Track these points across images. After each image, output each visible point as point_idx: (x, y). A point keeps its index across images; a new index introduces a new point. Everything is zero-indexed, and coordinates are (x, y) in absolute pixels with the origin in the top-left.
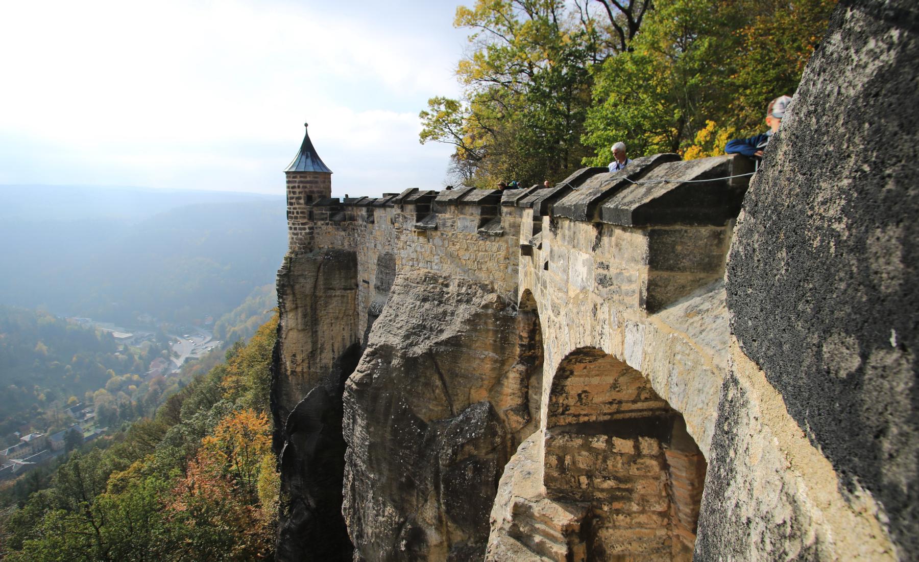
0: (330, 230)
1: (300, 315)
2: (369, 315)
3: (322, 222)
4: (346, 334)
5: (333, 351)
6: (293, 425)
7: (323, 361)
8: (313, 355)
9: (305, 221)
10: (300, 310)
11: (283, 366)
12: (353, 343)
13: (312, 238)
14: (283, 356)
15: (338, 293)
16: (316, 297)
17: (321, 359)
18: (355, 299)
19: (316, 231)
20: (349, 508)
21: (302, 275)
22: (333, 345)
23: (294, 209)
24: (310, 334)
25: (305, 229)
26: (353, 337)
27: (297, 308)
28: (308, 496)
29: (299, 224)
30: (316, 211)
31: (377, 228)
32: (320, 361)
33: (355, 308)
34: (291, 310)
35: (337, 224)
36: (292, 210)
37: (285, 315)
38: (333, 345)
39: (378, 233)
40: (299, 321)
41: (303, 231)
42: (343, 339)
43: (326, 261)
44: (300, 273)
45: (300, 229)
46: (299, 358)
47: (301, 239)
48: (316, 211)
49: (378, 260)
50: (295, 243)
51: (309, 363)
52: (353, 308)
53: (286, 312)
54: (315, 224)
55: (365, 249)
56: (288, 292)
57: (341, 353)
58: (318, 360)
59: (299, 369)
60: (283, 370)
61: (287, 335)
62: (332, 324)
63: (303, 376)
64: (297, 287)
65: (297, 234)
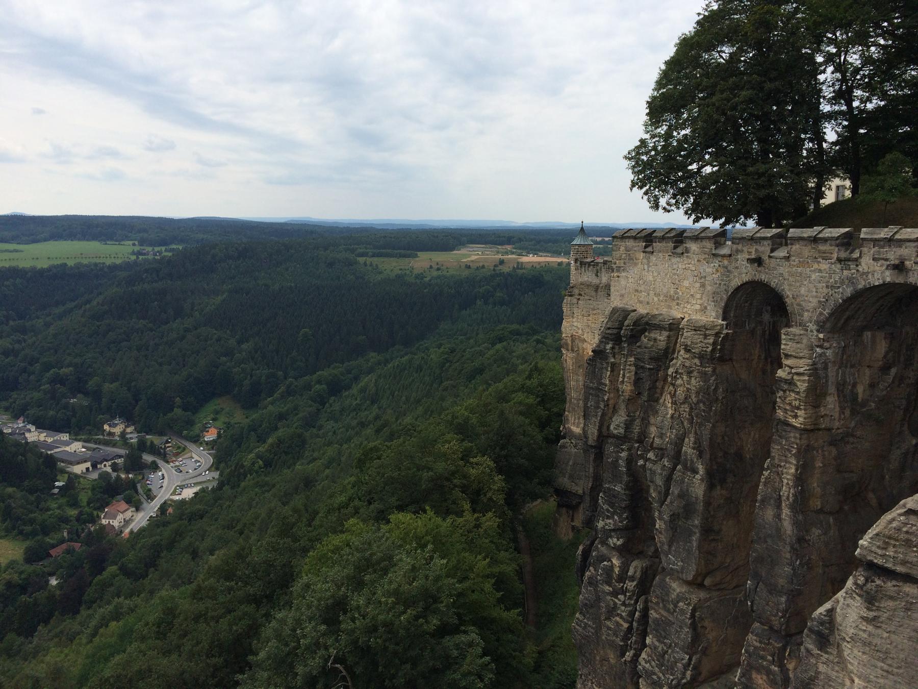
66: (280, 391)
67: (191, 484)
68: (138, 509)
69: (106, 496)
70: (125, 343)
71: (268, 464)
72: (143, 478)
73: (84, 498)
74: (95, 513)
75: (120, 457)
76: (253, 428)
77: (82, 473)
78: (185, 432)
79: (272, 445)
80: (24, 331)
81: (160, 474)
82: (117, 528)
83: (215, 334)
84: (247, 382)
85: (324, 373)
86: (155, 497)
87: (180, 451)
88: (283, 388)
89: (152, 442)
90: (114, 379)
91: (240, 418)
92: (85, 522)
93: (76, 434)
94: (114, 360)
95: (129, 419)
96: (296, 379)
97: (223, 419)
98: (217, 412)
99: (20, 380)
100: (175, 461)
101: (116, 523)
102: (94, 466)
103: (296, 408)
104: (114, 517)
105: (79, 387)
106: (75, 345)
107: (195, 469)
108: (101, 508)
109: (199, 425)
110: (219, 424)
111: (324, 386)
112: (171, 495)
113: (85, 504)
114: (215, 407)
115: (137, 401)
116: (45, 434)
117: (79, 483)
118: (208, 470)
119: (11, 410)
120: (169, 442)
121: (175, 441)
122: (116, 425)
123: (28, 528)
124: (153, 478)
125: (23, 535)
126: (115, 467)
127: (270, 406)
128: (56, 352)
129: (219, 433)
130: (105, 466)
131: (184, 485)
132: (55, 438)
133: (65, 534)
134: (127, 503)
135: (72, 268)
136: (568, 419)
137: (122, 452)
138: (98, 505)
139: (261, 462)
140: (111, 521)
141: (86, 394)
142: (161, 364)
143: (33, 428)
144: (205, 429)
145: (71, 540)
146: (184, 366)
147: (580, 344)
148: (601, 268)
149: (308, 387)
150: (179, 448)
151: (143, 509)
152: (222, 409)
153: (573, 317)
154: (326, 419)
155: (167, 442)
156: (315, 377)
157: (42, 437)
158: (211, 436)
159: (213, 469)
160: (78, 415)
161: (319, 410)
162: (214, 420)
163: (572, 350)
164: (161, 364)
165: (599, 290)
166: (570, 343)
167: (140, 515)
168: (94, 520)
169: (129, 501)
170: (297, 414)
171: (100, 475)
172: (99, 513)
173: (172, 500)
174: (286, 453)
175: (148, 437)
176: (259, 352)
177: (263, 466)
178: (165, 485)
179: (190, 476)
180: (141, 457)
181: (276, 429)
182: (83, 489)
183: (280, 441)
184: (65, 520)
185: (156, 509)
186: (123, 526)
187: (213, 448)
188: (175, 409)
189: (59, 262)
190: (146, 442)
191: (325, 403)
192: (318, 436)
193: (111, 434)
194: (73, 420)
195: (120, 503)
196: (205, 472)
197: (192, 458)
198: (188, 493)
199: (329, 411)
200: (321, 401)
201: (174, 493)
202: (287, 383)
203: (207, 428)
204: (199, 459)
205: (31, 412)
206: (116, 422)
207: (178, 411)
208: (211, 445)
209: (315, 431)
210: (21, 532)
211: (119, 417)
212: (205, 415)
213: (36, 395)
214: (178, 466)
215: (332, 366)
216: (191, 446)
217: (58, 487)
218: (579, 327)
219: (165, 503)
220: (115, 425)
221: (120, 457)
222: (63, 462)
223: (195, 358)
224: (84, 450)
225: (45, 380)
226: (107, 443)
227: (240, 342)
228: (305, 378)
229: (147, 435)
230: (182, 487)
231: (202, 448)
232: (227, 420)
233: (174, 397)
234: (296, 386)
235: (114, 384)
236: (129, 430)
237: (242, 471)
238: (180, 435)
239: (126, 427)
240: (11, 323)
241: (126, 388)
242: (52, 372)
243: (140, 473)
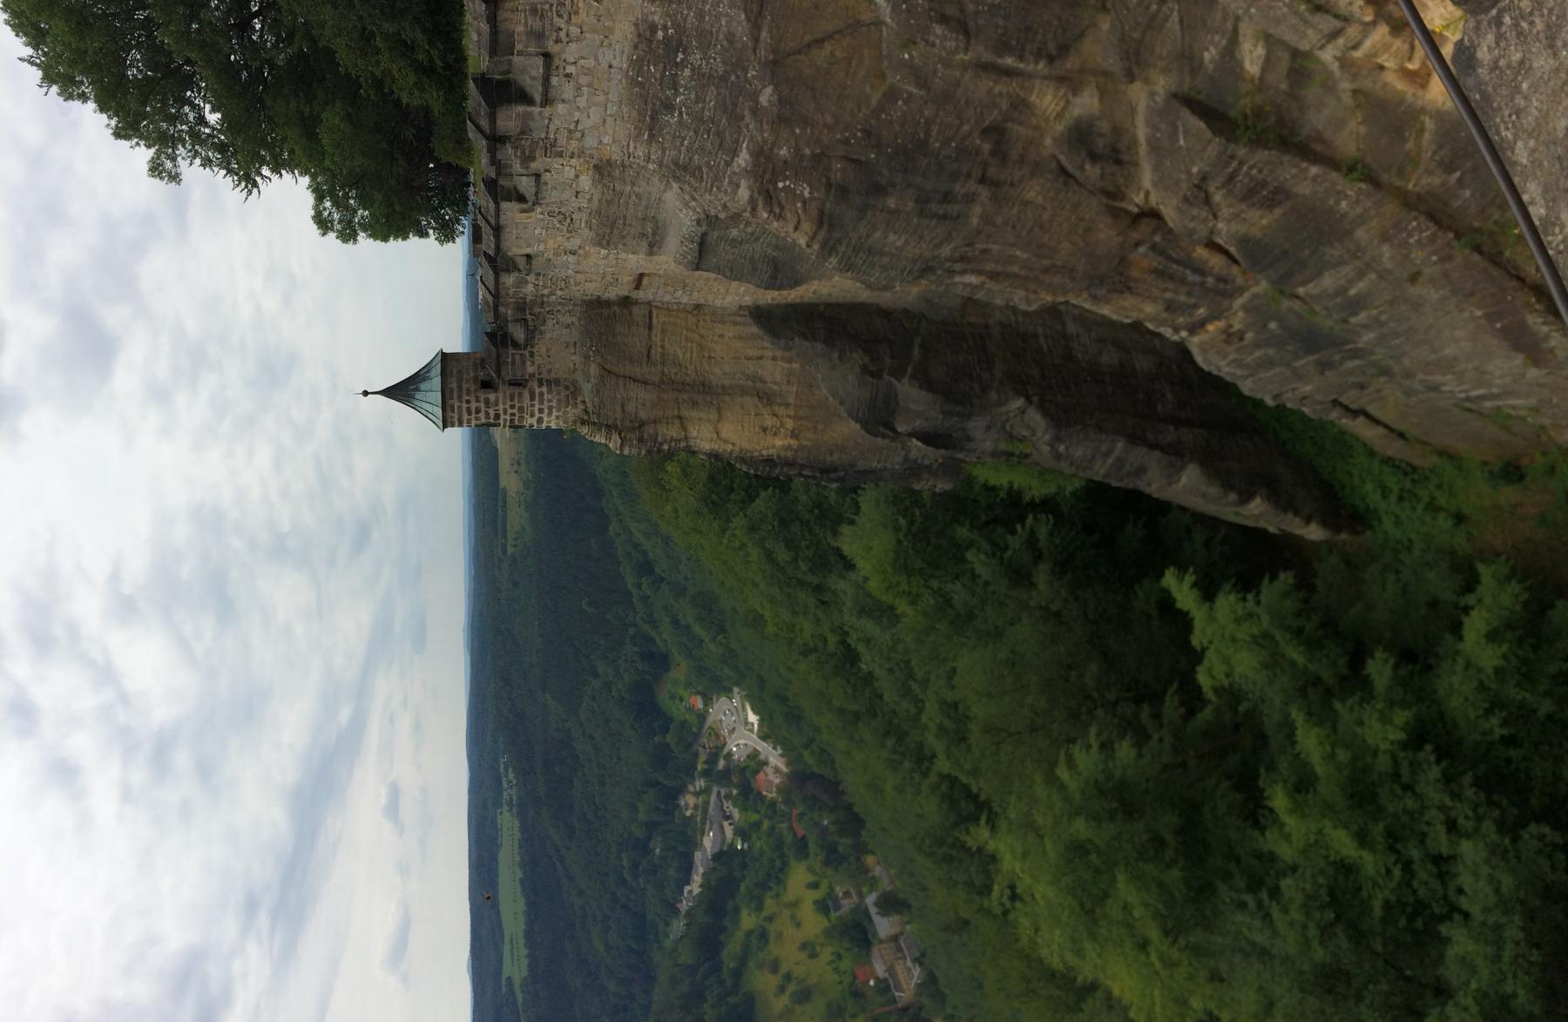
0: (543, 349)
1: (694, 414)
2: (697, 269)
3: (528, 363)
4: (730, 331)
5: (760, 358)
6: (881, 429)
7: (778, 377)
8: (766, 398)
9: (526, 394)
10: (684, 413)
11: (783, 453)
12: (749, 320)
13: (557, 382)
14: (764, 453)
15: (657, 339)
16: (662, 382)
17: (775, 383)
18: (669, 309)
19: (545, 376)
20: (1026, 289)
21: (623, 407)
22: (749, 359)
23: (505, 412)
24: (727, 398)
25: (541, 394)
26: (739, 319)
27: (680, 417)
28: (1003, 409)
29: (533, 406)
30: (508, 374)
31: (542, 247)
32: (778, 384)
33: (685, 311)
34: (685, 429)
35: (532, 334)
36: (508, 417)
37: (692, 442)
38: (749, 359)
39: (551, 244)
40: (703, 415)
41: (546, 397)
42: (739, 338)
43: (599, 359)
44: (618, 408)
45: (541, 402)
46: (769, 421)
47: (559, 401)
48: (508, 374)
49: (600, 245)
50: (566, 413)
51: (780, 405)
52: (681, 315)
53: (686, 438)
54: (532, 375)
55: (579, 277)
56: (651, 431)
57: (766, 344)
58: (775, 388)
59: (790, 424)
60: (789, 454)
61: (726, 442)
62: (710, 357)
63: (801, 418)
64: (643, 415)
65: (550, 408)
66: (650, 631)
71: (722, 629)
78: (694, 729)
81: (734, 749)
84: (640, 666)
85: (630, 580)
86: (755, 750)
88: (646, 627)
89: (705, 763)
91: (680, 670)
95: (680, 790)
97: (681, 692)
98: (672, 697)
108: (762, 798)
110: (685, 694)
111: (643, 579)
115: (658, 783)
123: (778, 863)
125: (783, 868)
127: (664, 636)
133: (784, 825)
139: (720, 637)
144: (691, 709)
149: (645, 598)
150: (710, 734)
152: (669, 692)
155: (704, 747)
156: (634, 591)
158: (699, 703)
159: (730, 695)
162: (681, 699)
167: (771, 759)
168: (773, 804)
173: (758, 731)
175: (699, 768)
185: (765, 745)
187: (711, 699)
189: (519, 889)
193: (696, 807)
198: (753, 718)
208: (708, 700)
210: (782, 870)
212: (676, 710)
216: (710, 721)
217: (743, 845)
220: (687, 804)
226: (705, 811)
227: (596, 675)
228: (635, 600)
230: (746, 723)
238: (697, 736)
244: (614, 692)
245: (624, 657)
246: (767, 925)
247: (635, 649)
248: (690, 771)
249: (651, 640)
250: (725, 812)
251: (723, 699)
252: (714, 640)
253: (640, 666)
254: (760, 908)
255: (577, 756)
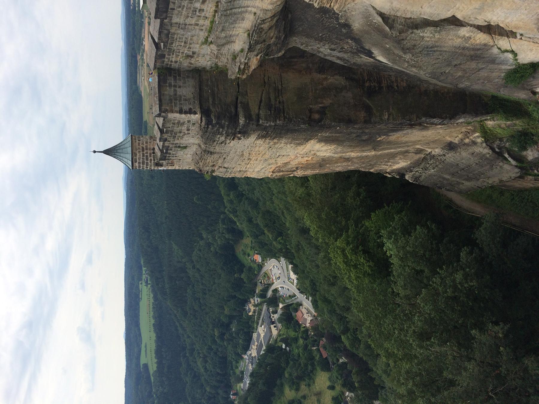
67: (288, 273)
68: (301, 305)
69: (292, 322)
70: (201, 301)
71: (280, 234)
72: (282, 298)
73: (292, 334)
74: (302, 329)
75: (268, 309)
76: (256, 236)
77: (277, 330)
79: (269, 231)
80: (193, 350)
81: (280, 289)
82: (312, 318)
83: (196, 252)
86: (294, 294)
87: (266, 275)
88: (231, 216)
89: (261, 291)
90: (222, 308)
91: (247, 241)
92: (308, 336)
93: (254, 328)
94: (211, 307)
95: (246, 301)
96: (226, 207)
97: (248, 251)
98: (244, 254)
99: (221, 355)
100: (272, 279)
101: (309, 319)
102: (273, 323)
103: (245, 212)
104: (306, 320)
105: (227, 326)
106: (202, 327)
107: (278, 269)
108: (299, 325)
109: (251, 264)
110: (251, 253)
112: (293, 285)
113: (296, 334)
114: (241, 254)
115: (235, 297)
116: (253, 346)
117: (283, 334)
118: (279, 262)
119: (238, 360)
120: (261, 281)
121: (260, 278)
122: (249, 308)
123: (310, 367)
124: (281, 292)
126: (275, 312)
128: (205, 337)
129: (257, 254)
130: (273, 317)
131: (288, 277)
132: (255, 341)
133: (314, 348)
134: (297, 311)
135: (155, 321)
136: (380, 170)
137: (265, 307)
138: (297, 327)
139: (279, 238)
140: (308, 321)
141: (230, 323)
142: (214, 283)
143: (249, 353)
144: (254, 261)
145: (318, 346)
146: (216, 270)
147: (290, 166)
148: (173, 144)
149: (231, 202)
150: (265, 276)
151: (301, 302)
152: (242, 250)
153: (246, 171)
154: (253, 195)
155: (261, 282)
157: (254, 347)
160: (243, 328)
161: (247, 198)
162: (249, 255)
163: (294, 171)
164: (214, 283)
165: (212, 150)
166: (281, 173)
168: (306, 331)
169: (296, 310)
170: (249, 212)
171: (279, 323)
172: (302, 326)
174: (274, 223)
175: (257, 292)
176: (208, 228)
177: (282, 237)
178: (287, 287)
179: (282, 271)
180: (269, 298)
181: (257, 224)
182: (287, 333)
183: (266, 226)
184: (306, 347)
185: (302, 295)
186: (311, 314)
188: (242, 277)
190: (261, 294)
191: (243, 193)
192: (265, 203)
193: (254, 312)
194: (245, 330)
195: (297, 315)
196: (281, 264)
197: (271, 270)
198: (293, 276)
199: (247, 192)
200: (240, 196)
201: (293, 283)
202: (228, 213)
203: (253, 260)
204: (272, 266)
205: (239, 351)
206: (248, 308)
207: (243, 276)
209: (261, 204)
210: (312, 372)
211: (245, 306)
212: (246, 260)
213: (230, 348)
214: (276, 278)
215: (218, 185)
216: (264, 269)
218: (263, 167)
219: (299, 289)
220: (250, 309)
221: (268, 309)
222: (270, 340)
223: (211, 264)
224: (263, 326)
225: (221, 343)
226: (260, 314)
227: (202, 238)
228: (225, 203)
229: (256, 292)
230: (289, 278)
231: (266, 264)
232: (249, 248)
233: (234, 278)
234: (230, 208)
235: (225, 308)
236: (252, 301)
237: (284, 250)
238: (256, 275)
239: (251, 303)
240: (187, 355)
241: (228, 302)
242: (217, 340)
243: (279, 299)
244: (212, 249)
245: (218, 230)
246: (302, 400)
247: (224, 226)
248: (252, 293)
249: (235, 223)
250: (271, 319)
251: (273, 260)
252: (276, 240)
253: (227, 236)
254: (297, 390)
255: (189, 276)
